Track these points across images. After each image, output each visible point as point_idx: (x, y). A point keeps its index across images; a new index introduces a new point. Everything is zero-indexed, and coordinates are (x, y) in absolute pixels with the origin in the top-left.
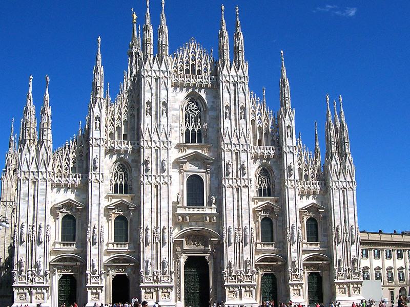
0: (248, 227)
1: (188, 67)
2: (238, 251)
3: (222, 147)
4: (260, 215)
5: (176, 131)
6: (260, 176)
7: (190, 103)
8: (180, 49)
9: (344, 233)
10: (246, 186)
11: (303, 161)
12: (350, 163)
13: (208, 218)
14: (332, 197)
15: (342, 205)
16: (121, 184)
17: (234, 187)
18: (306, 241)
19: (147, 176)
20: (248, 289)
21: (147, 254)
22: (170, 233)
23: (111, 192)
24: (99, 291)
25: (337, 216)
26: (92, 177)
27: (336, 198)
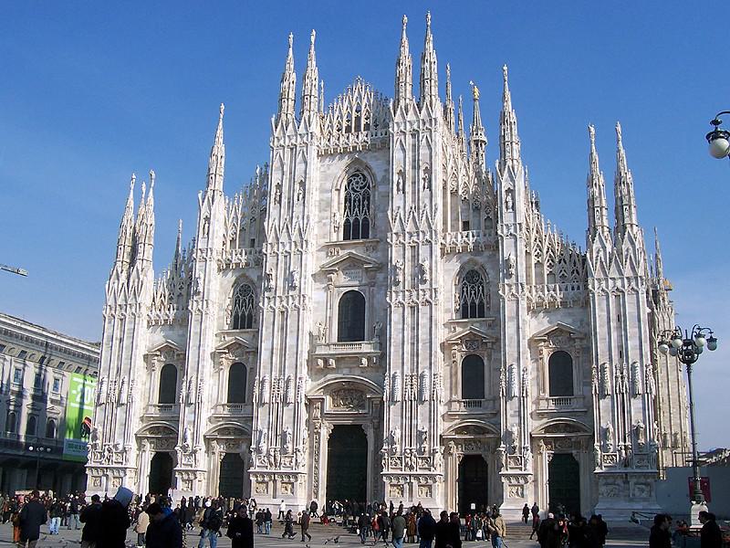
0: (427, 372)
3: (389, 240)
4: (460, 351)
5: (324, 224)
12: (633, 243)
13: (365, 361)
17: (406, 305)
18: (547, 396)
19: (269, 298)
20: (423, 482)
21: (261, 421)
22: (297, 388)
23: (226, 327)
24: (192, 477)
25: (602, 346)
26: (193, 306)
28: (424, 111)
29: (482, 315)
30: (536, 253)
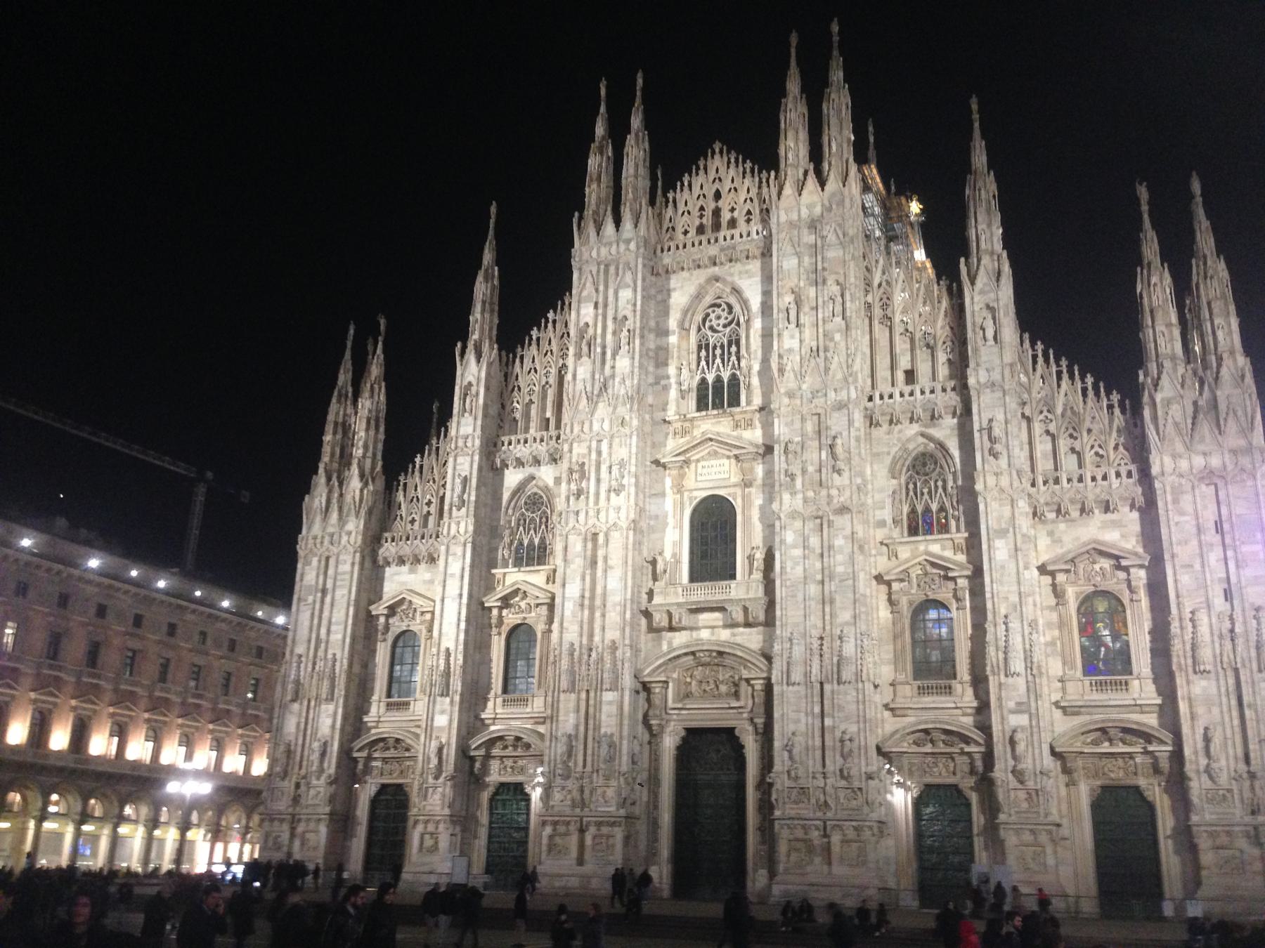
1: (704, 221)
2: (817, 709)
4: (907, 593)
6: (911, 477)
7: (710, 310)
8: (682, 185)
9: (1221, 637)
10: (843, 510)
11: (1059, 410)
12: (1237, 386)
14: (1161, 512)
15: (1211, 537)
16: (531, 541)
18: (1079, 673)
20: (851, 834)
27: (1182, 513)
28: (832, 184)
29: (944, 528)
30: (1041, 417)
